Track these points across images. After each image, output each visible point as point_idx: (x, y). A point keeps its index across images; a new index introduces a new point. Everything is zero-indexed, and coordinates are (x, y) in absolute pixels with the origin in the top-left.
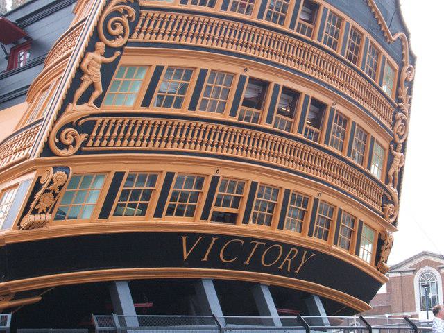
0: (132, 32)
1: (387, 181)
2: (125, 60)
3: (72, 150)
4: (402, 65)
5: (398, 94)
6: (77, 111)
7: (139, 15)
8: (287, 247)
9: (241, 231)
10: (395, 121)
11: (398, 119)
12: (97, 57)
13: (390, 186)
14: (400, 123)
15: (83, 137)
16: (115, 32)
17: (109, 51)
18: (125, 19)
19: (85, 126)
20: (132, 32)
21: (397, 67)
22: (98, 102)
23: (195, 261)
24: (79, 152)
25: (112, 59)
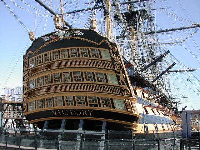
0: (29, 75)
1: (120, 84)
2: (30, 80)
3: (26, 98)
4: (109, 49)
5: (111, 57)
6: (25, 91)
7: (28, 71)
8: (81, 110)
9: (63, 108)
10: (114, 66)
11: (115, 65)
12: (25, 81)
13: (122, 86)
14: (116, 65)
15: (27, 96)
16: (25, 76)
17: (26, 80)
18: (26, 73)
19: (27, 94)
20: (29, 75)
21: (108, 50)
22: (28, 89)
23: (58, 115)
24: (28, 99)
25: (27, 81)
